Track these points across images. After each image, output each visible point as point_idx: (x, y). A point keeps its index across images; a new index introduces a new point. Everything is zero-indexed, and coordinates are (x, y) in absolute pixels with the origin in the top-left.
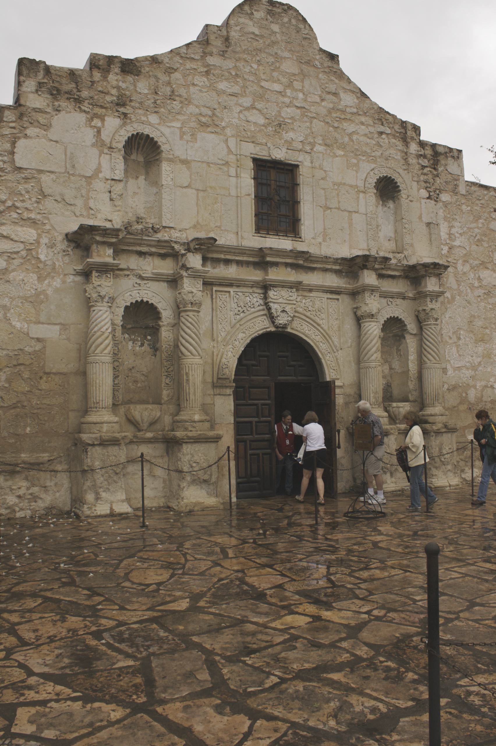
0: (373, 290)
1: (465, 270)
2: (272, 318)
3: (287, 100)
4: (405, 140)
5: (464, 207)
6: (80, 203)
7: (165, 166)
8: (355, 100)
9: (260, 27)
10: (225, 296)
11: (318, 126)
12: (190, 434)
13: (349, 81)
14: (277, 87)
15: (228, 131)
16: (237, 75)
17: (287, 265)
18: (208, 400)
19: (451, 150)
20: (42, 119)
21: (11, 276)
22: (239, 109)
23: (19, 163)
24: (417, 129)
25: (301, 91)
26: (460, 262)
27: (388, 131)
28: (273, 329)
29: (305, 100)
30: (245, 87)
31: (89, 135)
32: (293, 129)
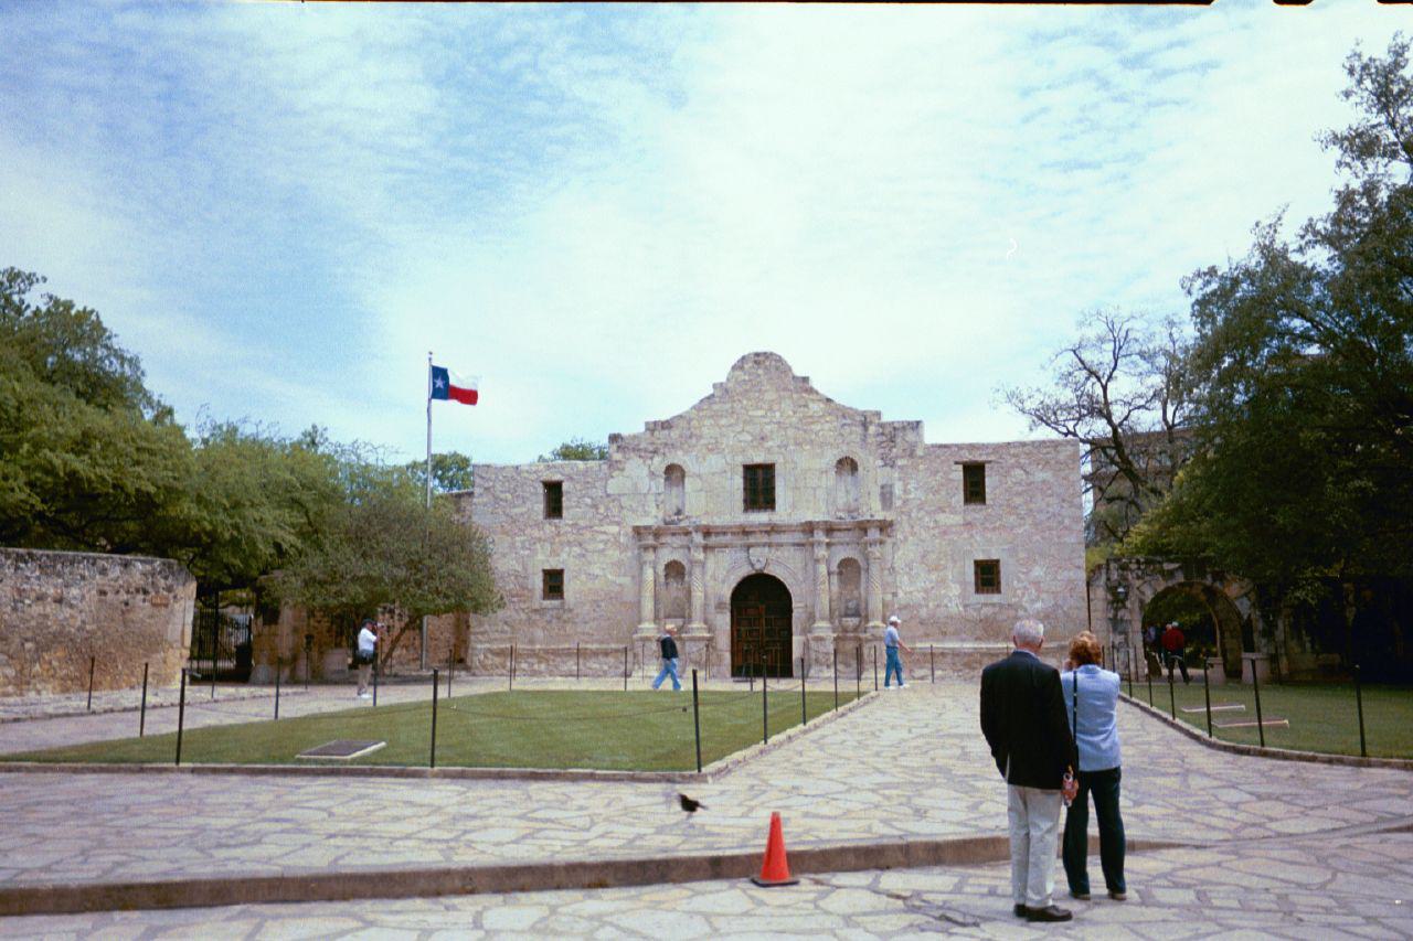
0: (819, 543)
1: (920, 516)
2: (752, 565)
3: (767, 420)
4: (865, 425)
5: (921, 467)
6: (640, 509)
7: (686, 480)
8: (822, 406)
9: (750, 374)
10: (721, 554)
11: (790, 432)
12: (689, 635)
13: (817, 393)
14: (761, 413)
15: (727, 451)
16: (733, 412)
17: (761, 532)
18: (711, 617)
19: (909, 423)
20: (620, 466)
21: (606, 553)
22: (732, 435)
23: (609, 491)
24: (878, 414)
25: (779, 410)
26: (914, 510)
27: (849, 421)
28: (754, 572)
29: (781, 416)
30: (738, 419)
31: (645, 472)
32: (773, 439)
